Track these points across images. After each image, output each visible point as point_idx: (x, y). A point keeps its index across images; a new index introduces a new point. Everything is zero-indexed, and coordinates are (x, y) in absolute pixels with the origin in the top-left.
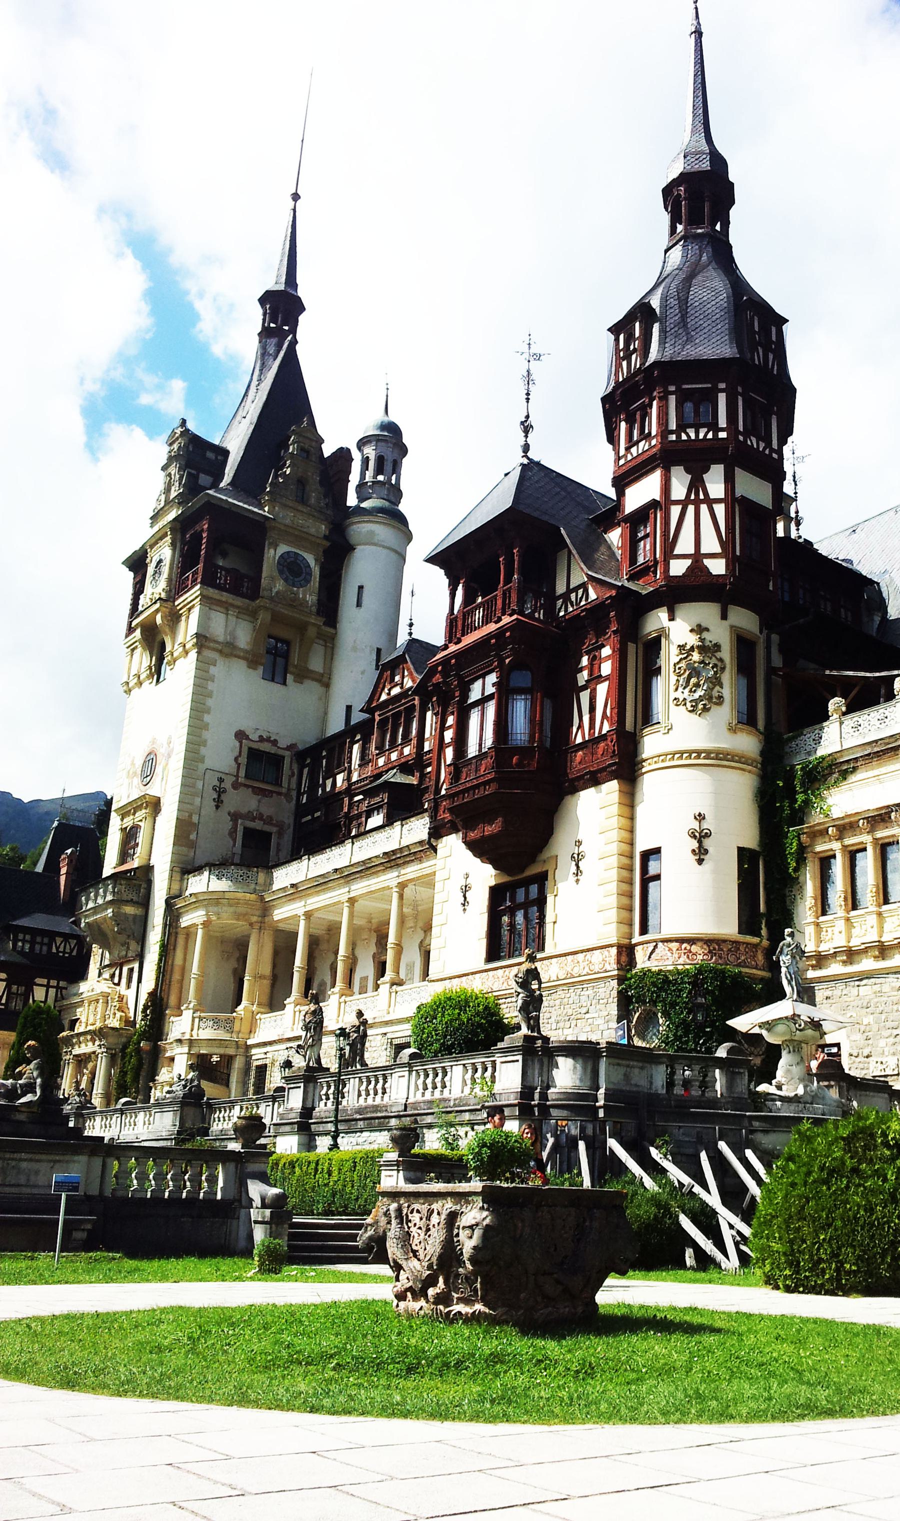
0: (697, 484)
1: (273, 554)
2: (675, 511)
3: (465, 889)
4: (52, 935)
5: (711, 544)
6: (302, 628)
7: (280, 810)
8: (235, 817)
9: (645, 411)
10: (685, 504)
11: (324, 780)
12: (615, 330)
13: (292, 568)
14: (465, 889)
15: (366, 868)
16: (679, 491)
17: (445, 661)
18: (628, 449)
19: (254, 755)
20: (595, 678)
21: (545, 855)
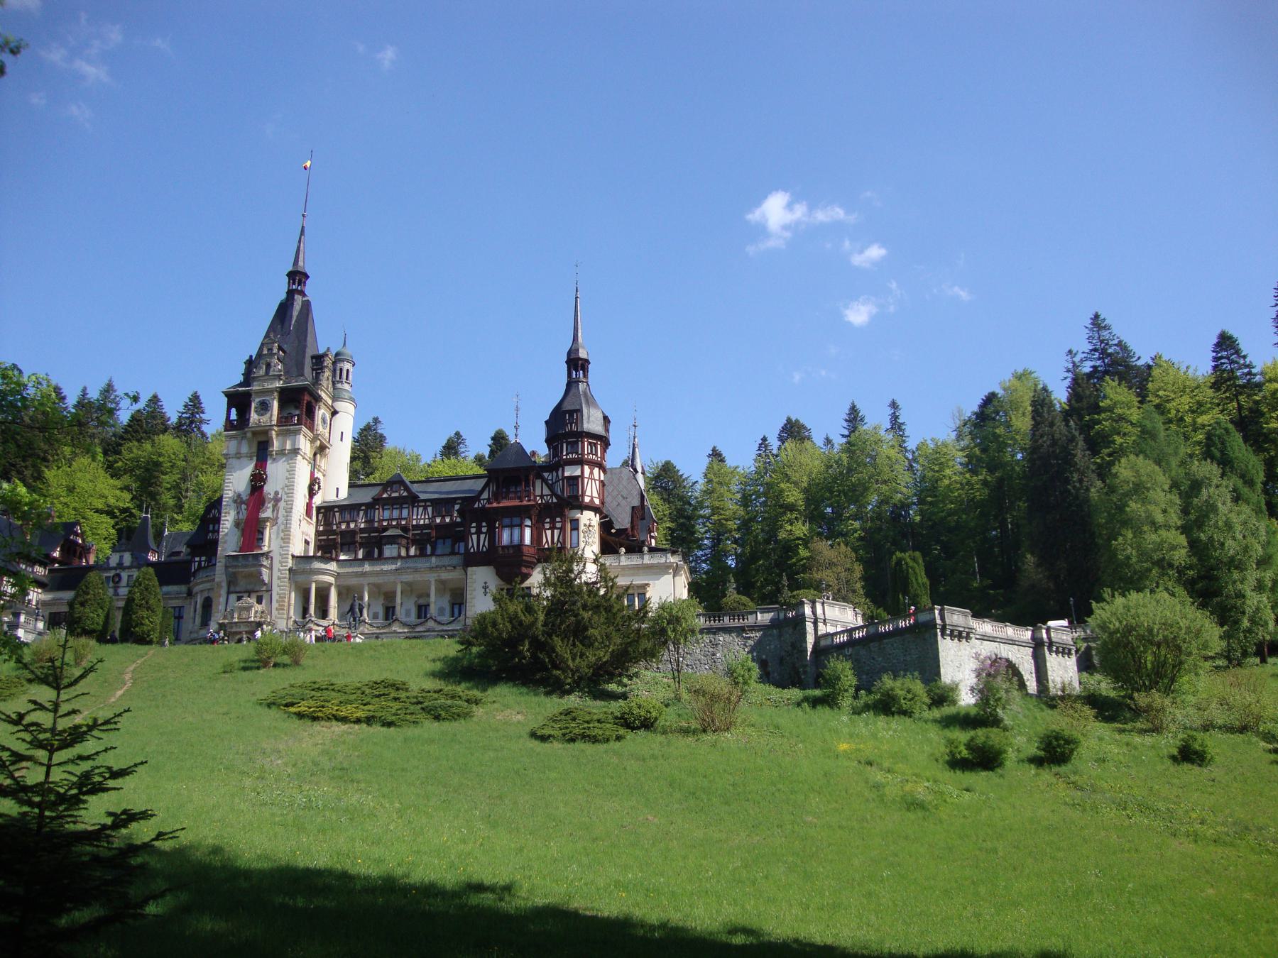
0: (591, 473)
5: (595, 494)
9: (577, 443)
13: (324, 421)
14: (485, 588)
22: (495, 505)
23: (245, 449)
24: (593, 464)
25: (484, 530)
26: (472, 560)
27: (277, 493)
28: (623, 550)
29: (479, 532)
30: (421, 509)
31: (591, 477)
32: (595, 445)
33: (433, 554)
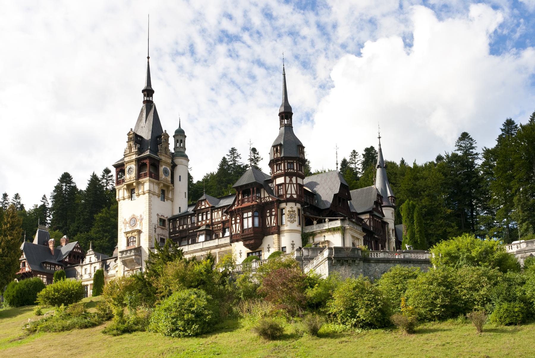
0: (291, 180)
1: (162, 169)
2: (287, 185)
3: (240, 253)
4: (55, 265)
5: (294, 192)
6: (168, 187)
7: (166, 233)
8: (158, 235)
9: (280, 164)
10: (289, 184)
11: (179, 226)
12: (274, 146)
13: (166, 172)
14: (240, 253)
15: (210, 248)
16: (288, 181)
17: (238, 209)
18: (277, 171)
19: (161, 219)
20: (271, 215)
21: (261, 247)
22: (239, 206)
23: (126, 194)
24: (291, 175)
25: (238, 221)
26: (234, 239)
27: (141, 216)
28: (315, 222)
29: (236, 223)
30: (216, 213)
31: (291, 183)
32: (293, 163)
33: (223, 237)
